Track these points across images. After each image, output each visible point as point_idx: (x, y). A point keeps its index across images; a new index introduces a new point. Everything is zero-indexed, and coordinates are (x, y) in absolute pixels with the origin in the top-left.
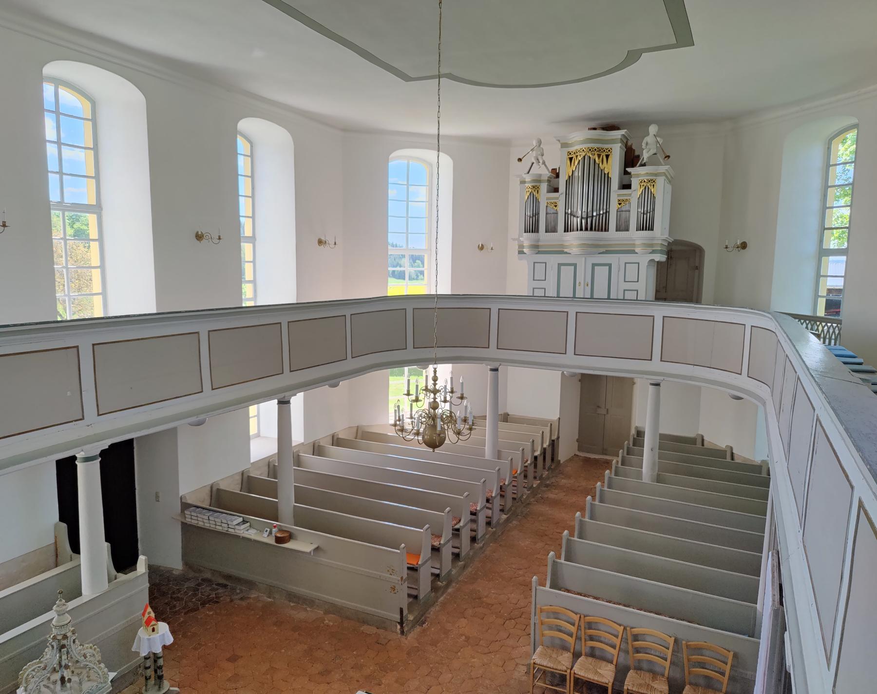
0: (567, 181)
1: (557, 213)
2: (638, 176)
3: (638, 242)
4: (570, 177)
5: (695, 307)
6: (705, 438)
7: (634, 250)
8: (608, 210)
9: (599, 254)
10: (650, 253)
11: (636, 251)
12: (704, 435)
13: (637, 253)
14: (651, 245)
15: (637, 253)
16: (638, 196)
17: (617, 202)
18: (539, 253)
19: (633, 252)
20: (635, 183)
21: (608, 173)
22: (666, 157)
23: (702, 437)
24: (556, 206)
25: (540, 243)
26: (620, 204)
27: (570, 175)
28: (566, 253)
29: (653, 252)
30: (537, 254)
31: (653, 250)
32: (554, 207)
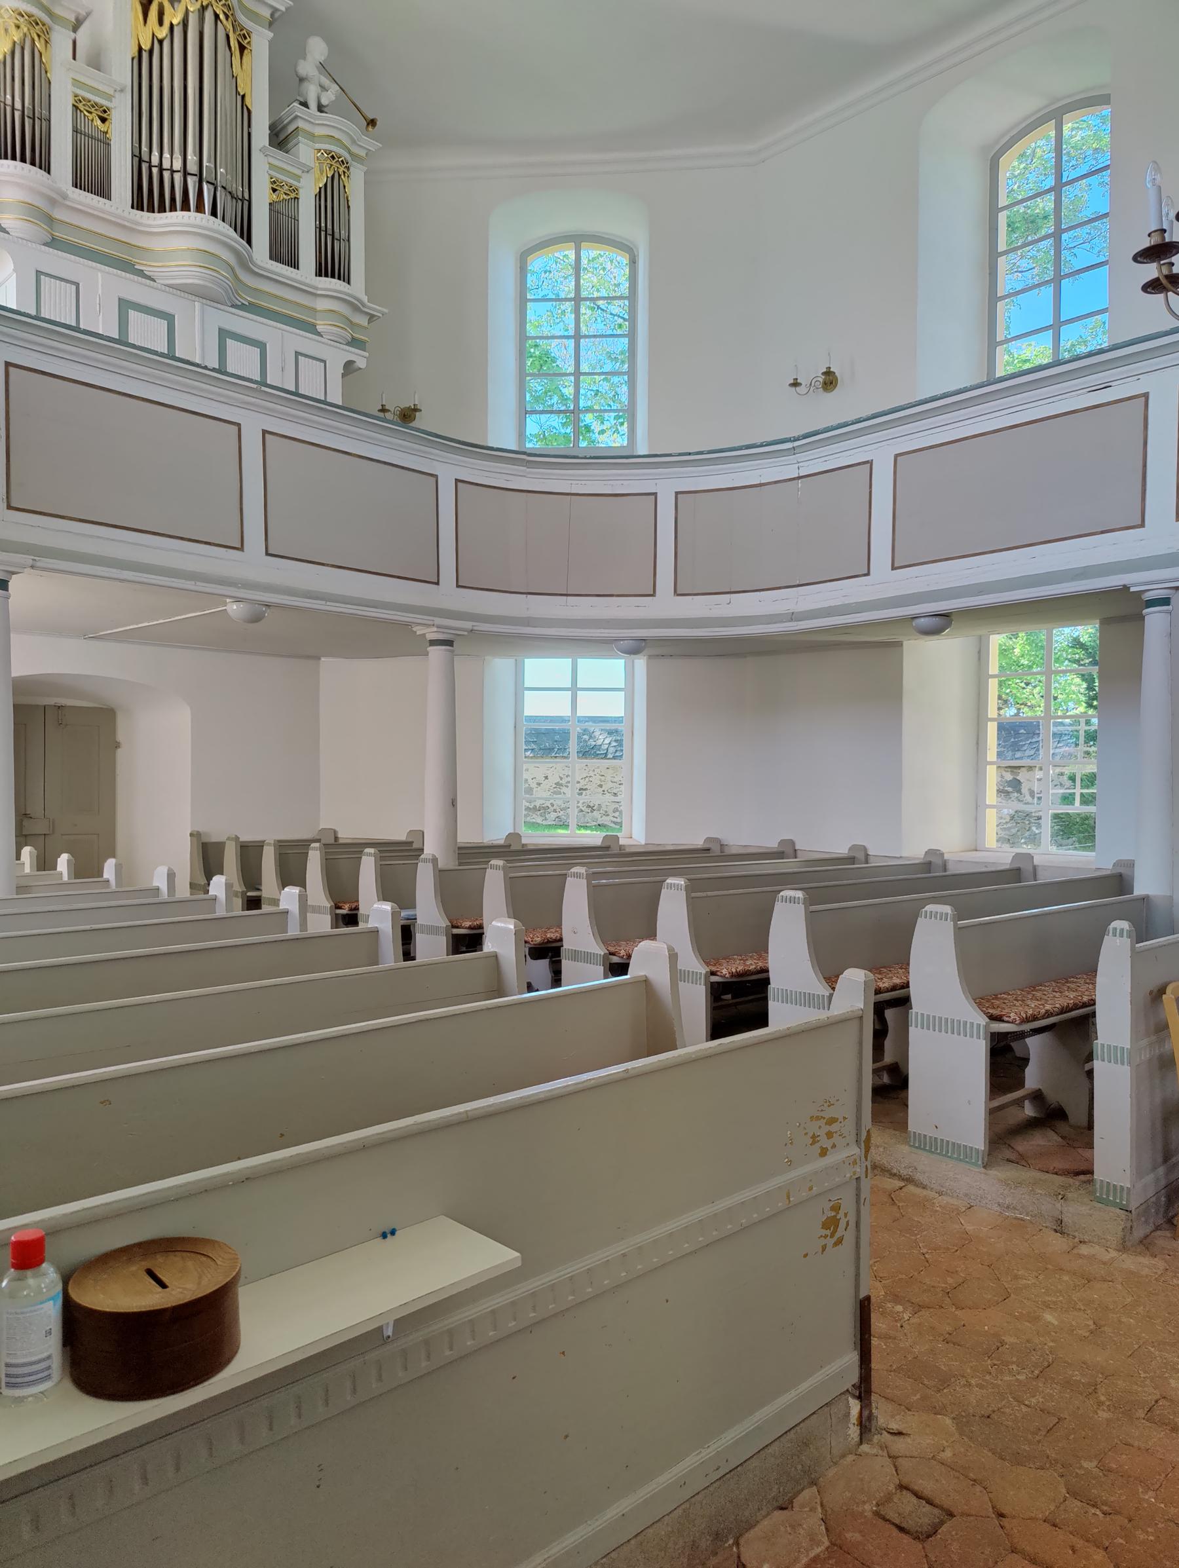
0: (133, 59)
1: (109, 145)
2: (311, 137)
3: (322, 305)
4: (140, 50)
5: (528, 461)
6: (339, 836)
7: (314, 326)
8: (246, 197)
9: (233, 306)
10: (348, 344)
11: (320, 328)
12: (337, 829)
13: (319, 334)
14: (352, 324)
15: (319, 334)
16: (318, 190)
17: (268, 186)
18: (53, 243)
19: (311, 328)
20: (305, 151)
21: (243, 97)
22: (368, 124)
23: (335, 832)
24: (103, 120)
25: (58, 214)
26: (274, 190)
27: (146, 46)
28: (141, 273)
29: (354, 342)
30: (46, 244)
31: (353, 339)
32: (99, 122)
